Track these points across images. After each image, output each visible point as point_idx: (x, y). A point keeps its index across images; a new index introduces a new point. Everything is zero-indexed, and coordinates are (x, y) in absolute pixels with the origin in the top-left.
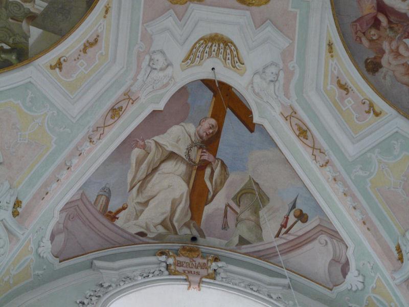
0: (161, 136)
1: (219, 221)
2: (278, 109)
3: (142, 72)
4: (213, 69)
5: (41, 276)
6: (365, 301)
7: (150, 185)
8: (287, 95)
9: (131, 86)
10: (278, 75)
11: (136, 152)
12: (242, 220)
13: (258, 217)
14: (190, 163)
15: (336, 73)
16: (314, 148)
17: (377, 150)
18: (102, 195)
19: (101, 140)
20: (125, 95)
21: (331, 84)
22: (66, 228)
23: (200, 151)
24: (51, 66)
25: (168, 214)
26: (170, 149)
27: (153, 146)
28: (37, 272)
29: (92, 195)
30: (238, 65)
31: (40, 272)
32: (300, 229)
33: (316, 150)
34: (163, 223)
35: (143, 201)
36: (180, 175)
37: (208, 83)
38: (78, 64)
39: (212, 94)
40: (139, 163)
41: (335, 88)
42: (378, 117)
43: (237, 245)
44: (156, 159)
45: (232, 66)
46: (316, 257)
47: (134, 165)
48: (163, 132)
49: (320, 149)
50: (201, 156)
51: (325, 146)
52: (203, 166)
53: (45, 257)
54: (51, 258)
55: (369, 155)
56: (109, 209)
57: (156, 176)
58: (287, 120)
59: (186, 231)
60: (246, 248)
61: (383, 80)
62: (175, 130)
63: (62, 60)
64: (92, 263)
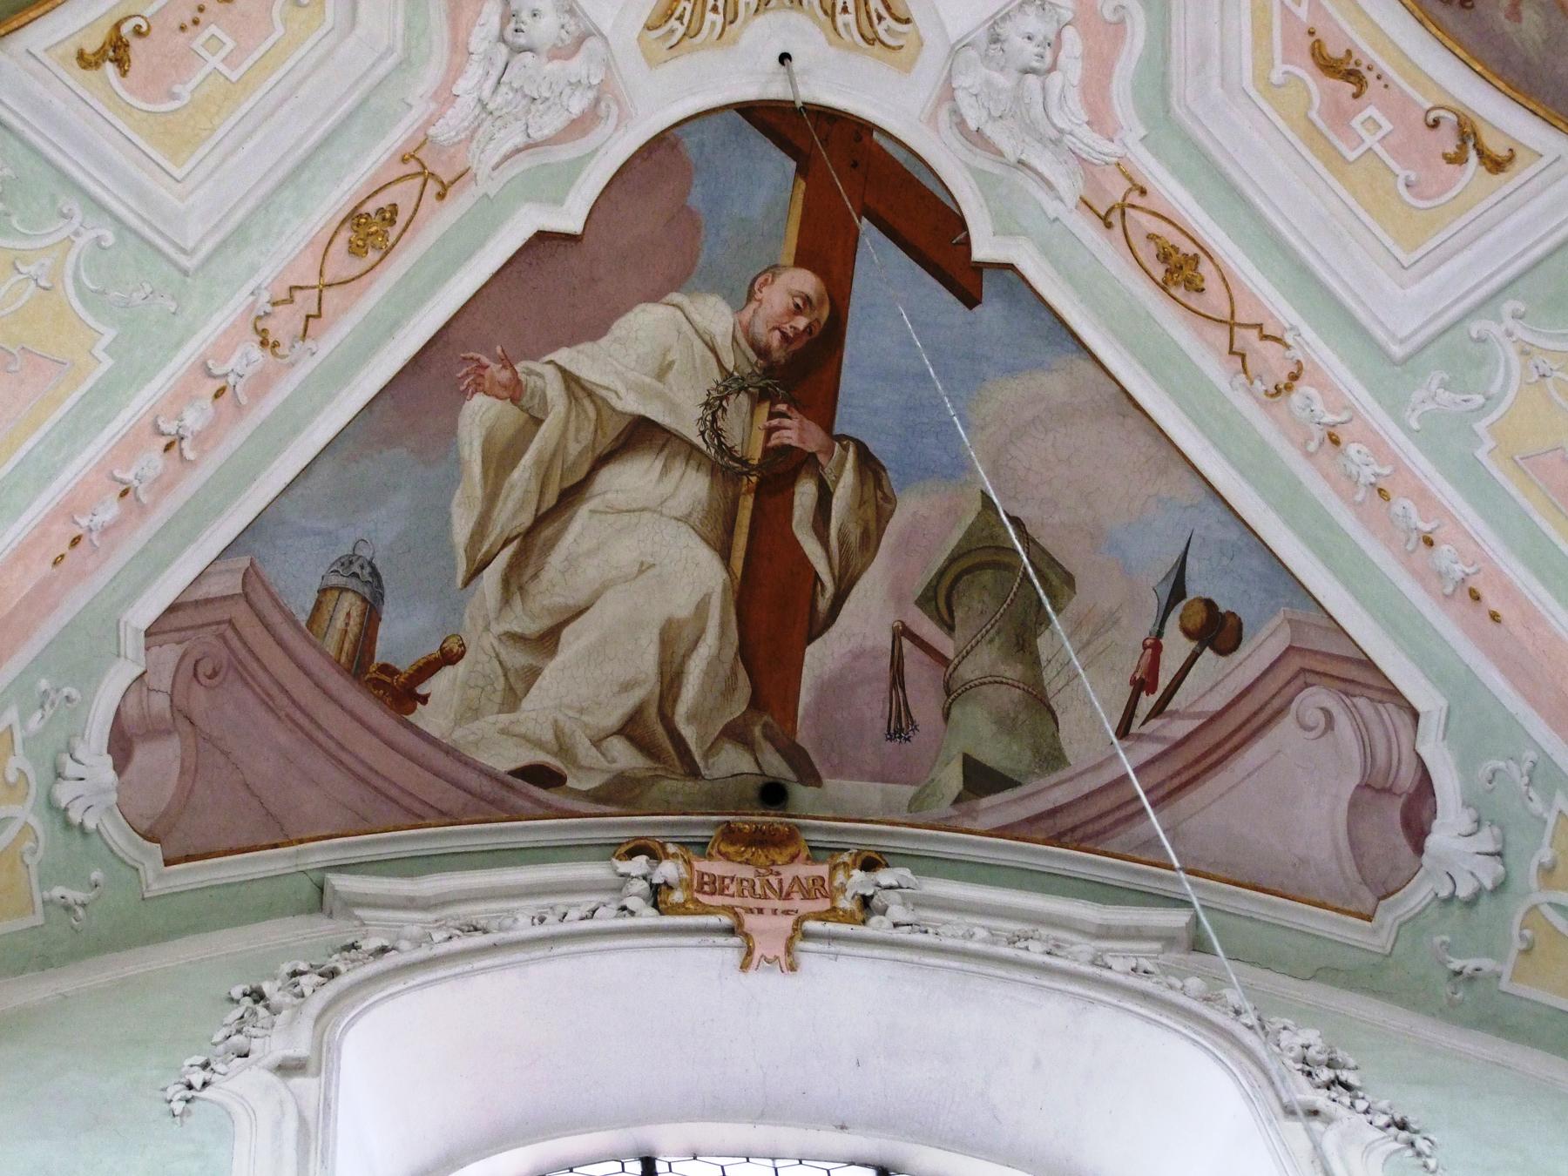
0: (587, 347)
1: (873, 707)
2: (1069, 185)
3: (474, 71)
4: (784, 58)
5: (80, 912)
6: (1515, 932)
7: (556, 559)
8: (1099, 118)
9: (430, 122)
10: (1055, 44)
11: (481, 414)
12: (968, 687)
13: (1035, 662)
14: (724, 466)
15: (1302, 12)
16: (1231, 324)
17: (1508, 306)
18: (342, 590)
19: (309, 343)
20: (404, 160)
21: (1284, 62)
22: (182, 714)
23: (764, 409)
24: (81, 56)
25: (648, 688)
26: (631, 404)
27: (554, 389)
28: (58, 891)
29: (298, 579)
30: (887, 30)
31: (75, 895)
32: (1213, 682)
33: (1237, 331)
34: (631, 729)
35: (532, 627)
36: (684, 519)
37: (775, 121)
38: (197, 44)
39: (793, 164)
40: (501, 459)
41: (1307, 74)
42: (1502, 176)
43: (958, 800)
44: (574, 449)
45: (863, 36)
46: (1297, 786)
47: (476, 468)
48: (594, 329)
49: (1260, 326)
50: (769, 431)
51: (1283, 311)
52: (782, 469)
53: (90, 824)
54: (119, 836)
55: (1475, 327)
56: (381, 654)
57: (582, 515)
58: (1109, 226)
59: (733, 761)
60: (998, 808)
61: (1509, 26)
62: (647, 327)
63: (126, 29)
64: (322, 890)
